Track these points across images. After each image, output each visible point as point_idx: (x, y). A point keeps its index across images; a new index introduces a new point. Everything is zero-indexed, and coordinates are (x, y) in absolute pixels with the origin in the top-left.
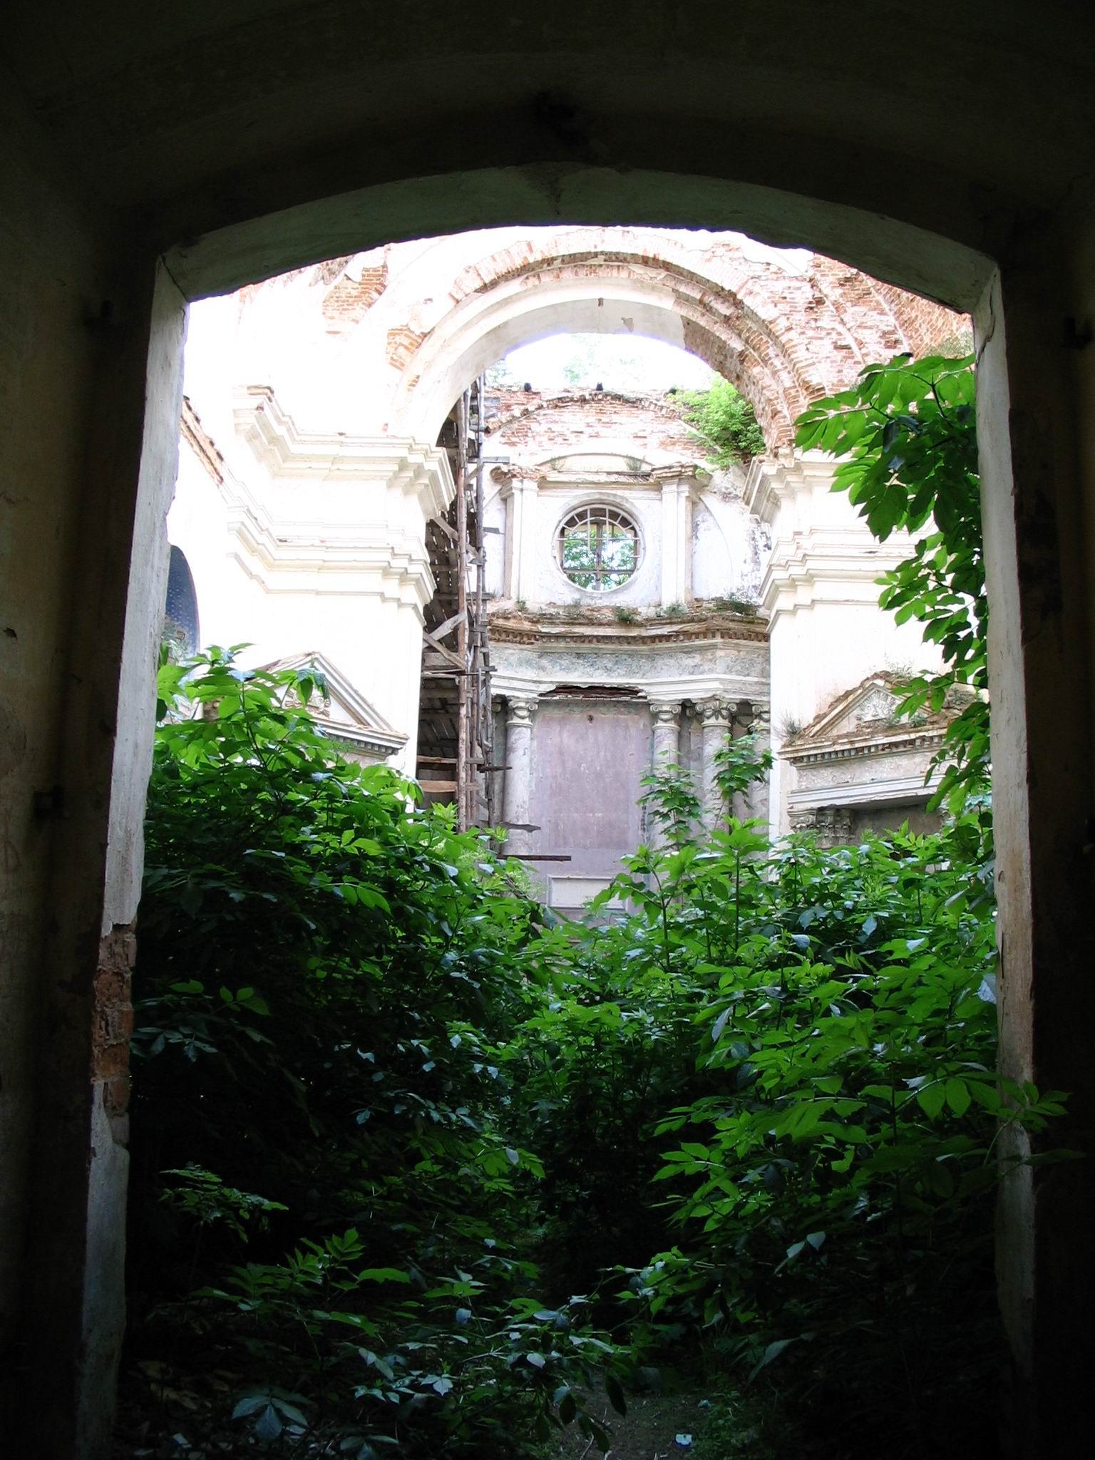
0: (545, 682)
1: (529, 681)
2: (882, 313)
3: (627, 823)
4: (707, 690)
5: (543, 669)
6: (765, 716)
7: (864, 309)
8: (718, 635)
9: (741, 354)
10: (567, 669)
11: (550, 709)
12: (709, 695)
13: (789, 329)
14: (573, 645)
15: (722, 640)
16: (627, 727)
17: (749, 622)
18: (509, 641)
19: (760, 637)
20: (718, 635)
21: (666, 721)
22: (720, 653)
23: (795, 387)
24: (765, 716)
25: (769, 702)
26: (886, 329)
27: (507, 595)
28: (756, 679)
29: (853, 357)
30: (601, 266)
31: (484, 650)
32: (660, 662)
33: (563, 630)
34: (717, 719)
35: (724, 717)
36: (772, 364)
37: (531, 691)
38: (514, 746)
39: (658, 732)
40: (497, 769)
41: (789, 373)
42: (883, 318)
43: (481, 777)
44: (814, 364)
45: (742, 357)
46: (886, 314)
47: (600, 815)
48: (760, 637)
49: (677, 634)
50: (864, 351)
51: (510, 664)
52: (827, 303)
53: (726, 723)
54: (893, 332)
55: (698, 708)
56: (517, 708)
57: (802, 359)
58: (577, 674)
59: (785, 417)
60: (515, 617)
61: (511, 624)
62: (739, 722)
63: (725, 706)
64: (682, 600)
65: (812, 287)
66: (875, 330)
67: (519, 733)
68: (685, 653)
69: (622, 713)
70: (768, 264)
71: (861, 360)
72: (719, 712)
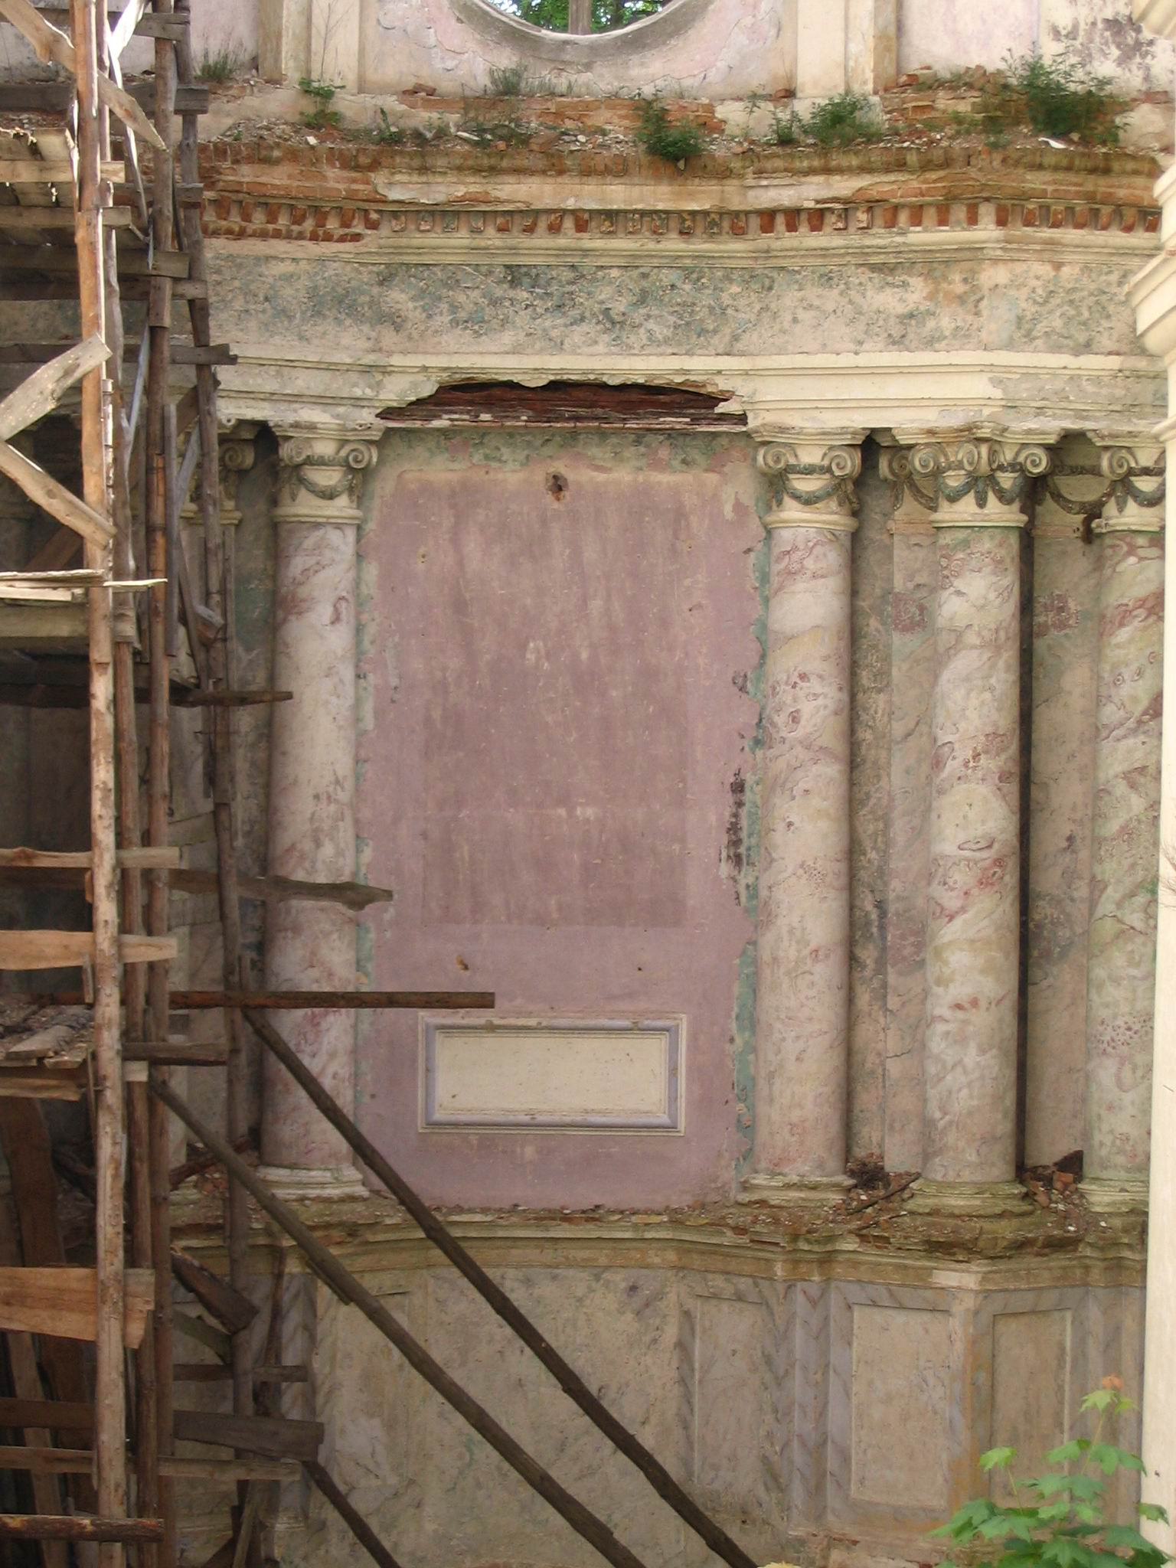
0: (404, 371)
1: (349, 368)
3: (683, 840)
4: (947, 405)
5: (395, 321)
6: (1146, 485)
8: (987, 213)
10: (475, 323)
11: (420, 451)
12: (956, 420)
14: (491, 238)
17: (1093, 171)
18: (277, 235)
19: (1130, 214)
20: (987, 213)
21: (809, 500)
22: (994, 275)
24: (1146, 485)
25: (1157, 538)
27: (267, 64)
31: (191, 290)
33: (460, 191)
34: (981, 502)
35: (1003, 497)
37: (357, 402)
38: (303, 592)
39: (785, 536)
40: (243, 700)
43: (191, 718)
47: (590, 812)
48: (1130, 214)
49: (847, 207)
51: (284, 313)
53: (1010, 516)
55: (917, 460)
56: (309, 461)
58: (508, 338)
60: (293, 156)
61: (279, 178)
62: (1058, 497)
63: (1007, 456)
64: (865, 84)
67: (318, 547)
68: (874, 268)
69: (657, 465)
72: (991, 479)
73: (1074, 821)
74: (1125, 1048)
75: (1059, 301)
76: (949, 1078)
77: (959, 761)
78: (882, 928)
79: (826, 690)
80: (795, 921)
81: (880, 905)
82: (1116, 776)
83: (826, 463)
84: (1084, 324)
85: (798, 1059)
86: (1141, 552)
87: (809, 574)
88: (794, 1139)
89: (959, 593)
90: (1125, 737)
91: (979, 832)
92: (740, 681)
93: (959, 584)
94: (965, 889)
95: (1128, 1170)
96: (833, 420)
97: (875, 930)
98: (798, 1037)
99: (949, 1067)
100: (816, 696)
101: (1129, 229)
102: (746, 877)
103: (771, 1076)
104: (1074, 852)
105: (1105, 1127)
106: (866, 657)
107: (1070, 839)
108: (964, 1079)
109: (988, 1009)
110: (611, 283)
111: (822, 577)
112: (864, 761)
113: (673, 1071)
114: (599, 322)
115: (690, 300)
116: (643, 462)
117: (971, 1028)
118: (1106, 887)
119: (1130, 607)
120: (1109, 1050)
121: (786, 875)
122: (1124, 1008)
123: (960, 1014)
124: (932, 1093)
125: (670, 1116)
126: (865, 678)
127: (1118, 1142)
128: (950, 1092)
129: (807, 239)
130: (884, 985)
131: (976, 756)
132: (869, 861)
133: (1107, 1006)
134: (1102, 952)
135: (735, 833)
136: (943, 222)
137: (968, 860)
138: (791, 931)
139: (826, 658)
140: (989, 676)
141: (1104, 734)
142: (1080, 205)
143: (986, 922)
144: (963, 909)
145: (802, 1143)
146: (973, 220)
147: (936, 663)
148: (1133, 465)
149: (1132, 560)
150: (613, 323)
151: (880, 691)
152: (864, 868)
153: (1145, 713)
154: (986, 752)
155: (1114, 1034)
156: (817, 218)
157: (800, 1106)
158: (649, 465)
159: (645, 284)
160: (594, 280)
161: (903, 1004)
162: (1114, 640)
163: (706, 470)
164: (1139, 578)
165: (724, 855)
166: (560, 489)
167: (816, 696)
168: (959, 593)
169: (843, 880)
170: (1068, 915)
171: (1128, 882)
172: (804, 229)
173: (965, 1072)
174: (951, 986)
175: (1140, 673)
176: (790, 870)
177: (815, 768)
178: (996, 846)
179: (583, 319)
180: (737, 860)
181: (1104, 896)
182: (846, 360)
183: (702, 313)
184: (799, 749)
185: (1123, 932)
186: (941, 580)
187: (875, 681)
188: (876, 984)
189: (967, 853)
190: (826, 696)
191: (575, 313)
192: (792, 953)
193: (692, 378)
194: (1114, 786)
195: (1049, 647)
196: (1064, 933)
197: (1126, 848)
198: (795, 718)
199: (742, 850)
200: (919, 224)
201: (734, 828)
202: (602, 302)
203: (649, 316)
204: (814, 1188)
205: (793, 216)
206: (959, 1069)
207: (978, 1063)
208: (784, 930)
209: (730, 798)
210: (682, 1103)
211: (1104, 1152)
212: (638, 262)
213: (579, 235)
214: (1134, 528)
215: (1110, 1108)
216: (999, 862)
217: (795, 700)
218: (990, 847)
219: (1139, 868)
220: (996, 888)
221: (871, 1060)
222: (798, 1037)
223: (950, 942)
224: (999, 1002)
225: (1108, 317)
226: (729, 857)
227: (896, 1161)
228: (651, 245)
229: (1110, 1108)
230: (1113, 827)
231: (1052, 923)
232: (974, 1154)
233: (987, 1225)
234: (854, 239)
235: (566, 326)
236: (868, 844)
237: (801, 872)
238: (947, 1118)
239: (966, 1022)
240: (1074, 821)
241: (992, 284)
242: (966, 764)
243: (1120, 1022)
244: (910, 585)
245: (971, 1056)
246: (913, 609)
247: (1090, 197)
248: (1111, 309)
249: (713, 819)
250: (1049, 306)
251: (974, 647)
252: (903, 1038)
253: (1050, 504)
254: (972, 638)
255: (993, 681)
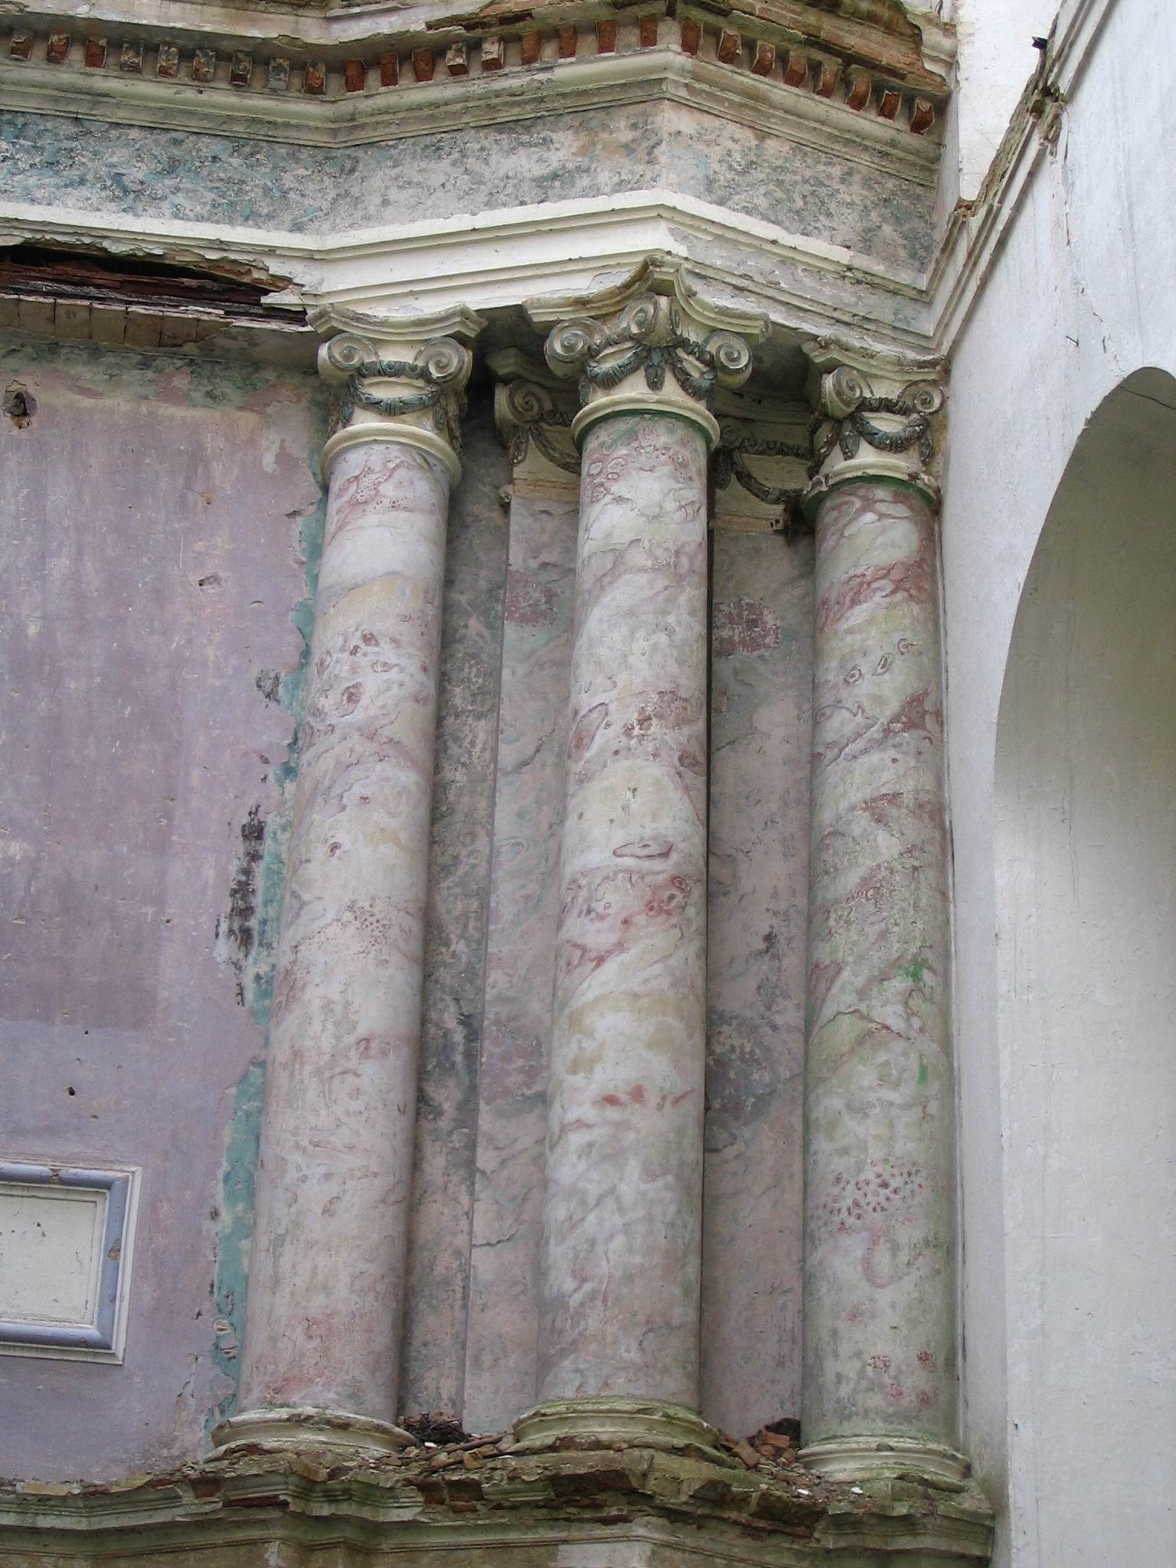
3: (160, 901)
15: (682, 60)
16: (196, 460)
21: (390, 410)
22: (671, 119)
28: (844, 256)
32: (377, 177)
34: (655, 384)
35: (685, 382)
55: (556, 345)
62: (746, 479)
68: (501, 127)
69: (171, 396)
73: (776, 914)
74: (878, 1216)
75: (763, 176)
76: (592, 1218)
77: (617, 728)
78: (471, 1056)
79: (403, 662)
80: (334, 990)
81: (466, 1021)
82: (853, 808)
83: (420, 363)
84: (797, 212)
85: (325, 1211)
86: (882, 507)
87: (386, 501)
88: (312, 1344)
89: (619, 500)
90: (865, 751)
91: (648, 832)
92: (268, 684)
93: (618, 488)
94: (623, 916)
95: (888, 1418)
96: (432, 307)
97: (458, 1058)
98: (328, 1176)
99: (592, 1200)
100: (387, 667)
101: (857, 103)
102: (256, 964)
103: (279, 1242)
104: (775, 957)
105: (845, 1348)
106: (461, 670)
107: (769, 938)
108: (618, 1220)
109: (660, 1107)
110: (127, 145)
111: (406, 509)
112: (452, 811)
113: (113, 1252)
114: (105, 188)
115: (237, 177)
116: (150, 390)
117: (632, 1135)
118: (839, 971)
119: (868, 578)
120: (851, 1221)
121: (322, 922)
122: (876, 1152)
123: (612, 1113)
124: (559, 1253)
125: (100, 1327)
126: (459, 696)
127: (869, 1370)
128: (593, 1243)
129: (412, 93)
131: (645, 721)
132: (454, 955)
133: (845, 1151)
134: (834, 1070)
135: (244, 897)
137: (630, 872)
138: (327, 1007)
139: (407, 618)
140: (664, 612)
141: (830, 755)
142: (798, 56)
143: (657, 969)
144: (620, 946)
145: (325, 1352)
146: (649, 40)
148: (867, 394)
149: (869, 517)
150: (126, 191)
151: (479, 716)
152: (445, 964)
153: (896, 719)
154: (660, 717)
155: (859, 1195)
157: (326, 1289)
158: (157, 394)
159: (176, 152)
160: (105, 138)
161: (503, 1162)
162: (844, 625)
163: (240, 408)
164: (880, 540)
165: (224, 927)
166: (25, 414)
167: (387, 667)
168: (619, 500)
169: (415, 947)
170: (768, 1049)
171: (877, 957)
173: (621, 1209)
174: (598, 1068)
175: (886, 664)
176: (331, 915)
177: (379, 767)
178: (674, 856)
179: (82, 182)
180: (245, 937)
181: (838, 983)
183: (254, 194)
184: (356, 741)
185: (871, 1033)
187: (473, 702)
188: (457, 1140)
189: (628, 862)
190: (402, 670)
191: (74, 174)
192: (327, 1043)
193: (232, 256)
194: (849, 823)
195: (736, 672)
196: (760, 1077)
197: (870, 907)
198: (352, 696)
199: (253, 923)
200: (572, 55)
201: (243, 890)
202: (114, 166)
203: (178, 189)
204: (344, 1426)
206: (610, 1204)
207: (644, 1194)
208: (316, 1005)
209: (240, 847)
210: (123, 1309)
211: (844, 1391)
212: (171, 123)
213: (89, 70)
214: (871, 472)
215: (854, 1315)
216: (677, 881)
217: (354, 670)
218: (665, 855)
219: (894, 938)
220: (674, 920)
221: (445, 1263)
222: (328, 1176)
223: (597, 1001)
224: (677, 1100)
225: (829, 215)
226: (231, 931)
228: (190, 94)
229: (854, 1315)
230: (850, 880)
231: (742, 1059)
232: (634, 1347)
233: (661, 1459)
234: (477, 85)
235: (58, 187)
236: (453, 930)
237: (348, 916)
238: (587, 1287)
239: (622, 1126)
240: (776, 914)
241: (674, 129)
242: (628, 731)
243: (869, 1174)
244: (534, 564)
245: (631, 1182)
246: (536, 595)
247: (813, 41)
248: (833, 207)
249: (210, 873)
250: (749, 178)
251: (643, 570)
252: (500, 1217)
253: (735, 487)
254: (638, 557)
255: (671, 619)
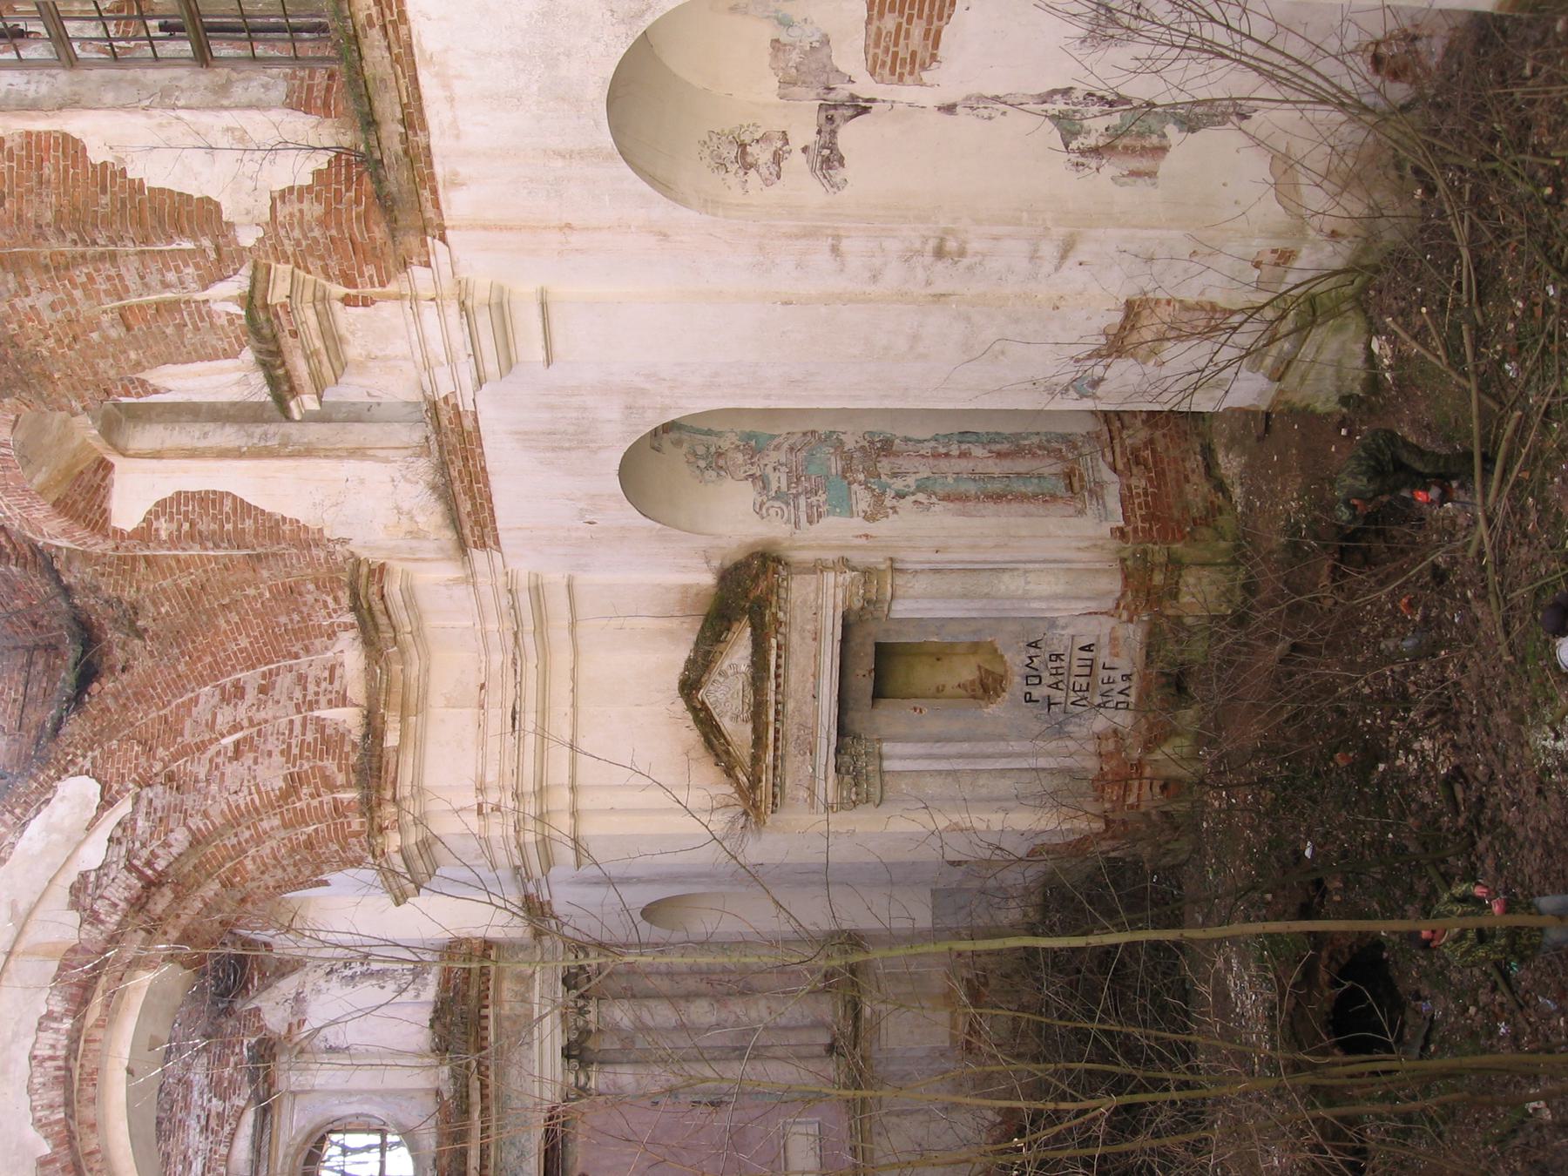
2: (195, 701)
7: (188, 723)
8: (484, 1012)
9: (224, 886)
13: (206, 815)
15: (491, 1007)
20: (484, 1012)
21: (589, 1078)
23: (282, 813)
26: (217, 698)
29: (252, 738)
30: (82, 1066)
36: (247, 841)
39: (602, 1087)
41: (262, 820)
42: (202, 700)
44: (257, 786)
45: (227, 884)
46: (198, 696)
50: (245, 723)
52: (174, 767)
53: (593, 1002)
54: (223, 689)
57: (248, 798)
59: (316, 830)
65: (150, 786)
66: (218, 710)
70: (110, 840)
71: (256, 729)
72: (580, 1009)
96: (559, 1069)
130: (762, 1046)
136: (486, 1028)
147: (645, 1029)
156: (484, 1086)
172: (488, 1091)
182: (537, 1064)
186: (617, 1029)
205: (484, 1086)
227: (826, 1039)
